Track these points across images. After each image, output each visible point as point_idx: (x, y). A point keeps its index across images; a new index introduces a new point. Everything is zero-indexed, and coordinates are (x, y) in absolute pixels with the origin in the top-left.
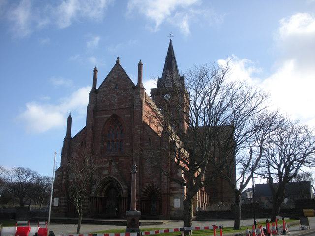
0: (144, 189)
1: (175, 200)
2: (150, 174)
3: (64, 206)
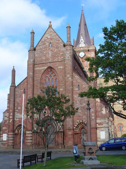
0: (76, 124)
1: (101, 132)
2: (80, 113)
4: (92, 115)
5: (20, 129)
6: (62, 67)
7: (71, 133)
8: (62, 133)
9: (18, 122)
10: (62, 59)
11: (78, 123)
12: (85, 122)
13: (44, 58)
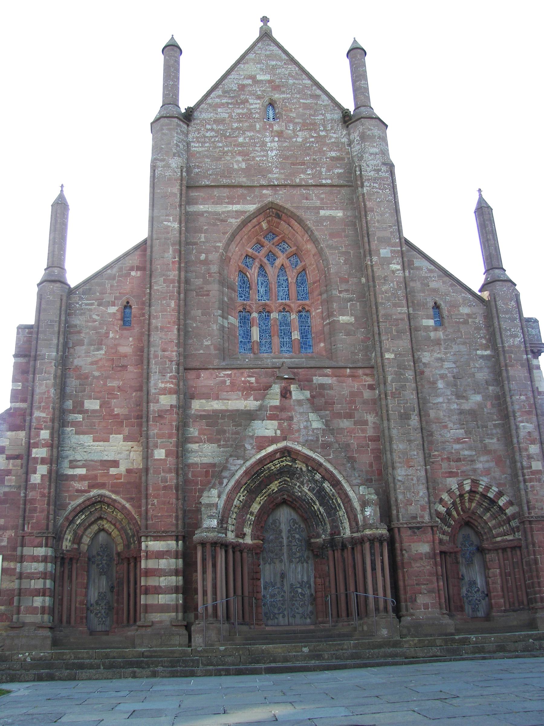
3: (42, 593)
4: (527, 450)
5: (86, 529)
6: (340, 214)
7: (424, 548)
8: (385, 544)
9: (82, 485)
10: (339, 175)
11: (450, 492)
12: (488, 488)
13: (239, 163)
